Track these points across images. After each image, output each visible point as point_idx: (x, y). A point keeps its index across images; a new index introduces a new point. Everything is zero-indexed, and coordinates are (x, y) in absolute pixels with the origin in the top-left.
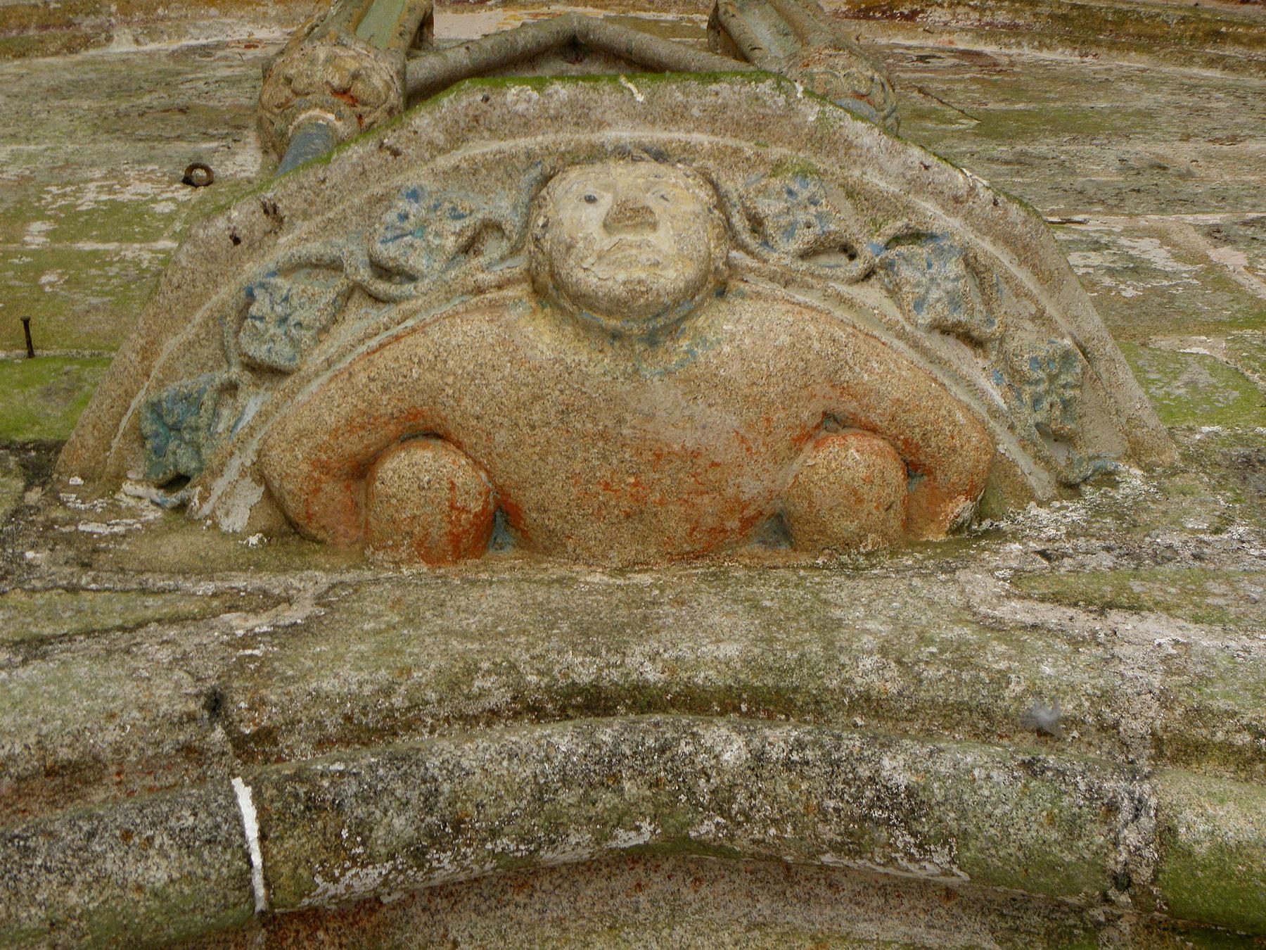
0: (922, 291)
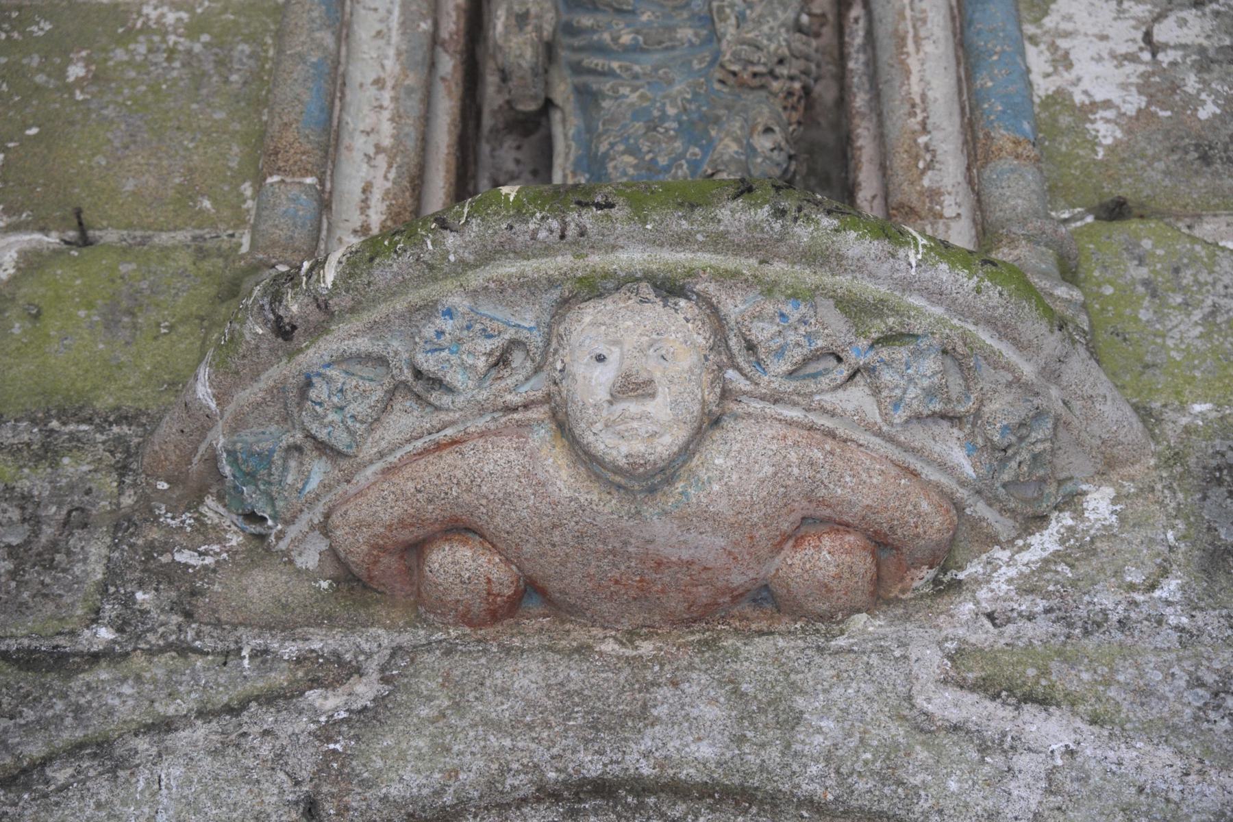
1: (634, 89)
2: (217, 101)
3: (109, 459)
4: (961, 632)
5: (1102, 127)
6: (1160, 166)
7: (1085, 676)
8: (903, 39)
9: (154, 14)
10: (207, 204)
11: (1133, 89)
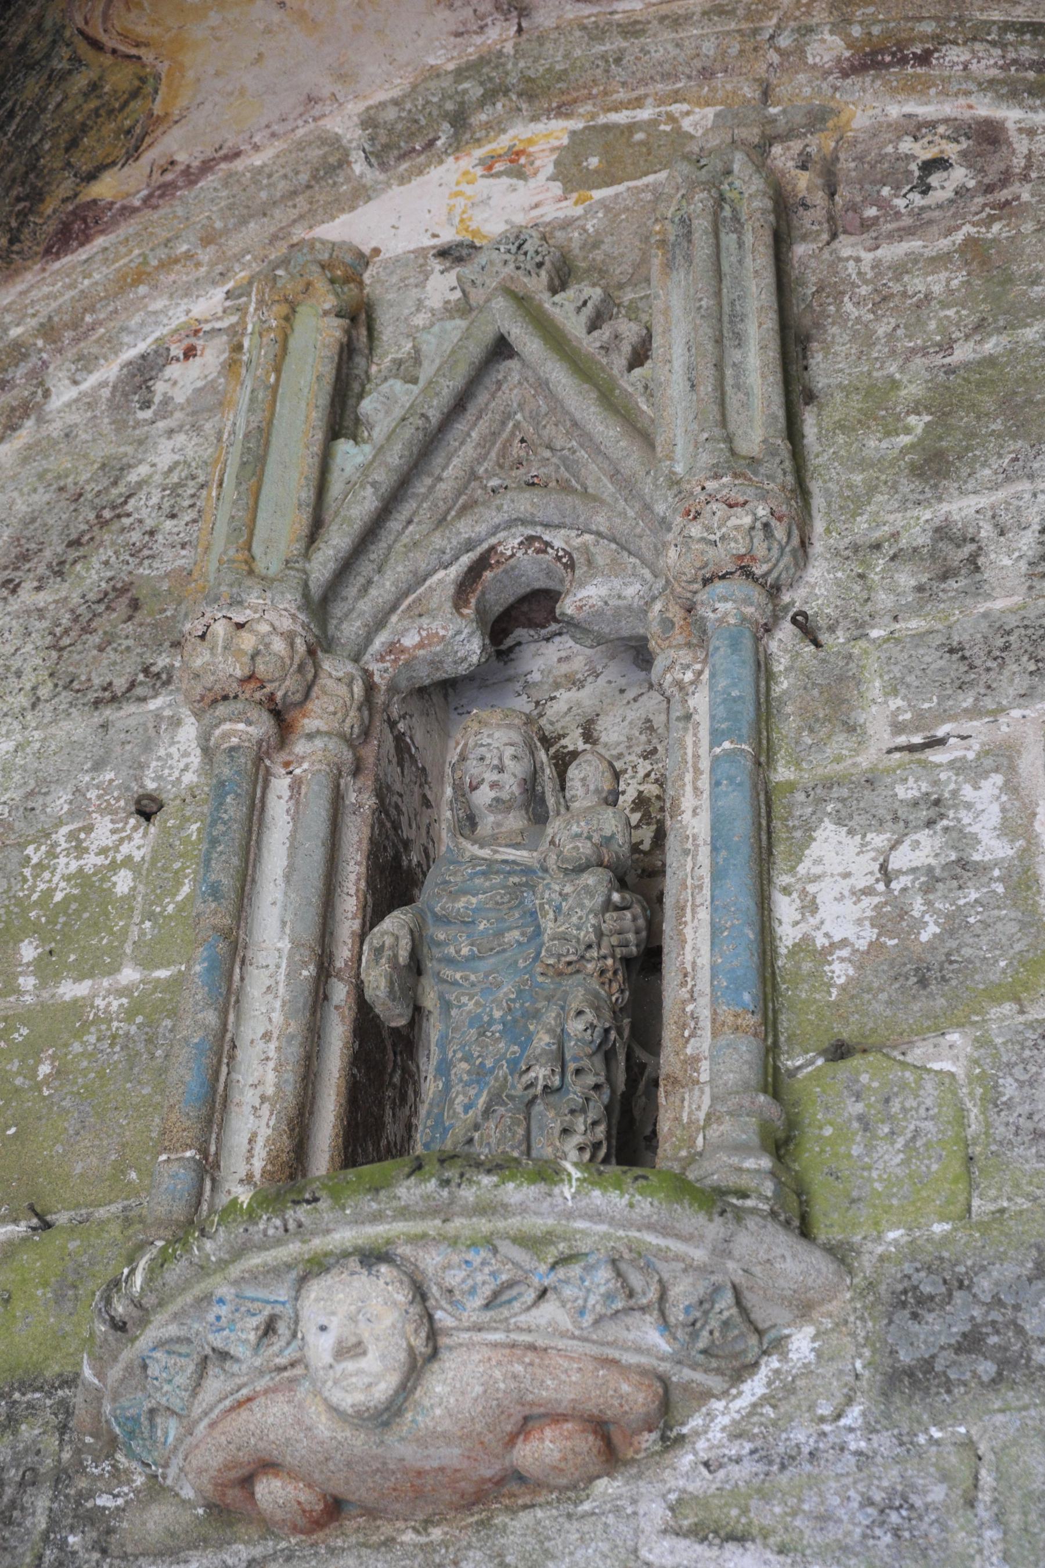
0: (580, 1302)
2: (145, 1077)
4: (681, 1483)
5: (837, 967)
6: (883, 996)
7: (777, 1510)
8: (683, 909)
11: (867, 923)
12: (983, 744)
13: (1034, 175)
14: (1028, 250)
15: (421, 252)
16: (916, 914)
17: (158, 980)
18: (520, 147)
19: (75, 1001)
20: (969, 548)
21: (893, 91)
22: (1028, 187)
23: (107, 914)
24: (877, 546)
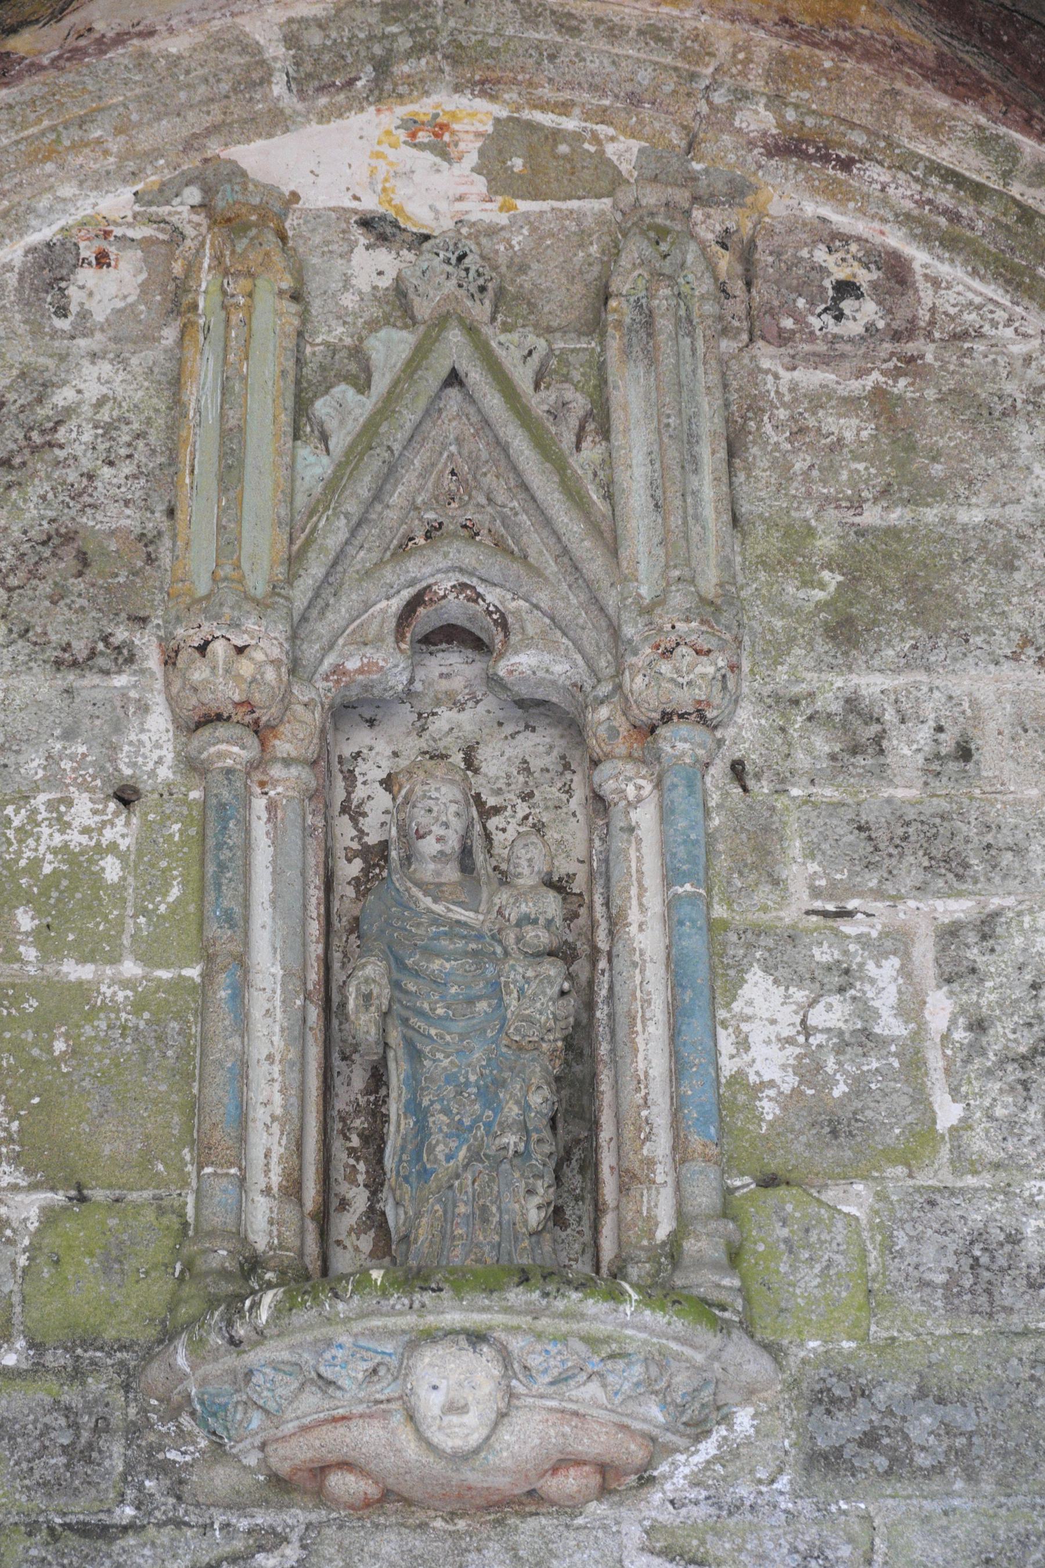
1: (447, 1057)
2: (159, 1074)
3: (118, 1380)
4: (653, 1514)
6: (803, 1139)
7: (727, 1546)
8: (634, 1019)
9: (109, 993)
10: (161, 1167)
12: (884, 926)
13: (937, 335)
14: (930, 420)
15: (342, 212)
16: (830, 1072)
17: (160, 979)
18: (443, 119)
19: (80, 983)
20: (874, 729)
21: (814, 190)
22: (932, 347)
23: (99, 899)
24: (795, 702)
